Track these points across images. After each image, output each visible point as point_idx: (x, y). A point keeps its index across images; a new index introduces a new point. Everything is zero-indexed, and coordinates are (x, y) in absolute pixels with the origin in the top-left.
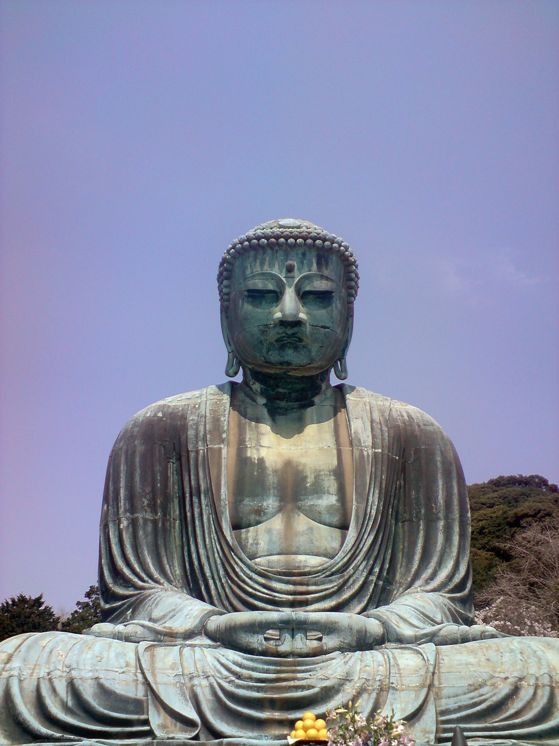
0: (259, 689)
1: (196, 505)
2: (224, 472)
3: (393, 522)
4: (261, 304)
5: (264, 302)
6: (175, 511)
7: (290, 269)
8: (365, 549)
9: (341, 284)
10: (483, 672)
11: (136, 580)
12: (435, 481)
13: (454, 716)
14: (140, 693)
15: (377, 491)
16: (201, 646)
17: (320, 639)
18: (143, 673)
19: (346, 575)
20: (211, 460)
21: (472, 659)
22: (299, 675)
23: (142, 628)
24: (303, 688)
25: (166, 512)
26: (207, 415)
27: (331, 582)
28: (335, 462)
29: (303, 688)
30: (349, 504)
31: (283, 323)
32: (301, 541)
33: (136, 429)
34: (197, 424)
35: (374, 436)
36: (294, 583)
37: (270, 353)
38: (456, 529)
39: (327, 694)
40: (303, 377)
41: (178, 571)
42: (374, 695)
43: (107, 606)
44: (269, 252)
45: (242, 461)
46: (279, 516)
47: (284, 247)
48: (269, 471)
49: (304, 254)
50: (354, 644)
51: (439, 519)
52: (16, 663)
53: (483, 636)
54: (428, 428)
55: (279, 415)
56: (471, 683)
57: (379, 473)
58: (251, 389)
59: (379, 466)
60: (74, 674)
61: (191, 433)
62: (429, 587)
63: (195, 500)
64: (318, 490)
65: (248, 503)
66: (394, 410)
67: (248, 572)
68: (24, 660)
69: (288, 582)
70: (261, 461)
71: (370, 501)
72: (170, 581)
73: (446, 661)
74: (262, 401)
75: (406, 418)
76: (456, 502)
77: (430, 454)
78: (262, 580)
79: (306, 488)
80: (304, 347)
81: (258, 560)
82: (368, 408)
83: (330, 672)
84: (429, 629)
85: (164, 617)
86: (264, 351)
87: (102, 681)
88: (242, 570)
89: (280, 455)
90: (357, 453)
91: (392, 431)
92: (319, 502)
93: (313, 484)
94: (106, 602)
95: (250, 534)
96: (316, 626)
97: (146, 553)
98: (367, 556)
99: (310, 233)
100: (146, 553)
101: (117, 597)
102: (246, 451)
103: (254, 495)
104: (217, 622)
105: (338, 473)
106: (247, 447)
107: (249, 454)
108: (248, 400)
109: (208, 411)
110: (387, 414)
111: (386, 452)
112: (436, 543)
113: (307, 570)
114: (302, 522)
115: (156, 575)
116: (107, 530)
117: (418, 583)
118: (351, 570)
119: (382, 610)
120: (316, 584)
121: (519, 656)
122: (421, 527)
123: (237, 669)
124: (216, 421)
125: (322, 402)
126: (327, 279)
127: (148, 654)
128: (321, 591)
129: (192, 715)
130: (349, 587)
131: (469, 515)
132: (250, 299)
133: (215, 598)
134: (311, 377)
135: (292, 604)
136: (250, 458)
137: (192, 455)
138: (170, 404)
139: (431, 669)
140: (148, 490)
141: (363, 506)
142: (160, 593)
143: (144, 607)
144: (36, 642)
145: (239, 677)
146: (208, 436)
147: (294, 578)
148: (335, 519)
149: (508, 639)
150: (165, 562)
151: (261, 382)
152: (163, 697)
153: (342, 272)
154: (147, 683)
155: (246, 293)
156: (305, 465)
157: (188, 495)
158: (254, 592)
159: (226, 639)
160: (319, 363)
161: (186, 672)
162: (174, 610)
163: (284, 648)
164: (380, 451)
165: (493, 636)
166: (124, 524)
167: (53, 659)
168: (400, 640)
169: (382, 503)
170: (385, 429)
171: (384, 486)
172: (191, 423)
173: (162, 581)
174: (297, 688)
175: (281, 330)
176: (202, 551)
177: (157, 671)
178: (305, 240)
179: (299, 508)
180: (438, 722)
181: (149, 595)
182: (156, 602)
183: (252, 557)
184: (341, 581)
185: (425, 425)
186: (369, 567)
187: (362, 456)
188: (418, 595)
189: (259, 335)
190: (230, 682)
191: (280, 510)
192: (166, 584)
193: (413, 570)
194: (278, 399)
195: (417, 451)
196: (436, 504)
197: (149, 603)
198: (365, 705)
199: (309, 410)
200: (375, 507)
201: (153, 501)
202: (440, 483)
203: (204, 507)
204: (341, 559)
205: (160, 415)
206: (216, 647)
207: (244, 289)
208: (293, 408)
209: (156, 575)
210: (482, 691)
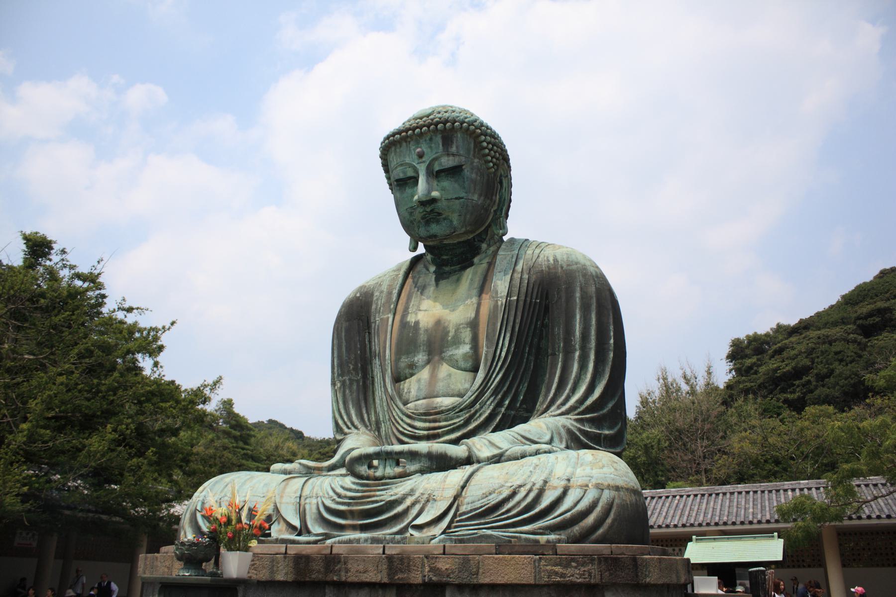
0: (348, 504)
2: (389, 337)
3: (532, 358)
9: (471, 156)
10: (495, 483)
12: (574, 316)
13: (464, 517)
15: (508, 335)
19: (473, 410)
22: (378, 493)
23: (298, 466)
24: (377, 502)
27: (458, 417)
28: (473, 315)
29: (377, 502)
31: (422, 203)
32: (440, 386)
36: (430, 421)
38: (592, 357)
40: (459, 243)
44: (404, 144)
45: (404, 324)
46: (428, 367)
47: (414, 137)
48: (422, 332)
49: (431, 139)
51: (575, 350)
54: (570, 268)
55: (443, 279)
56: (484, 491)
57: (512, 319)
59: (513, 313)
61: (374, 307)
62: (559, 412)
64: (457, 342)
65: (404, 361)
66: (542, 256)
67: (401, 415)
69: (425, 421)
71: (500, 345)
72: (366, 426)
75: (552, 261)
78: (408, 421)
80: (445, 219)
82: (514, 260)
86: (416, 229)
90: (492, 303)
91: (533, 278)
92: (456, 352)
93: (453, 337)
95: (405, 385)
96: (401, 454)
97: (351, 406)
98: (495, 392)
99: (432, 120)
100: (351, 406)
105: (474, 325)
107: (409, 319)
108: (424, 270)
110: (531, 263)
111: (522, 298)
114: (445, 369)
115: (356, 422)
117: (553, 408)
118: (477, 406)
120: (446, 420)
121: (531, 469)
124: (390, 293)
125: (481, 260)
126: (453, 155)
127: (284, 483)
128: (450, 425)
129: (297, 523)
130: (476, 420)
134: (467, 242)
135: (428, 438)
137: (373, 325)
139: (462, 483)
140: (352, 357)
144: (222, 479)
148: (469, 365)
149: (583, 452)
150: (364, 411)
153: (472, 145)
156: (449, 322)
160: (464, 229)
161: (304, 494)
163: (379, 473)
164: (515, 298)
165: (545, 452)
169: (513, 345)
170: (526, 276)
171: (517, 329)
173: (359, 426)
174: (373, 502)
175: (420, 210)
179: (443, 359)
183: (405, 403)
185: (568, 265)
186: (496, 401)
188: (537, 420)
190: (334, 500)
191: (428, 362)
192: (362, 429)
193: (549, 398)
194: (444, 265)
198: (414, 511)
199: (468, 270)
200: (505, 350)
201: (356, 365)
202: (578, 317)
204: (468, 398)
205: (358, 295)
208: (455, 271)
209: (356, 422)
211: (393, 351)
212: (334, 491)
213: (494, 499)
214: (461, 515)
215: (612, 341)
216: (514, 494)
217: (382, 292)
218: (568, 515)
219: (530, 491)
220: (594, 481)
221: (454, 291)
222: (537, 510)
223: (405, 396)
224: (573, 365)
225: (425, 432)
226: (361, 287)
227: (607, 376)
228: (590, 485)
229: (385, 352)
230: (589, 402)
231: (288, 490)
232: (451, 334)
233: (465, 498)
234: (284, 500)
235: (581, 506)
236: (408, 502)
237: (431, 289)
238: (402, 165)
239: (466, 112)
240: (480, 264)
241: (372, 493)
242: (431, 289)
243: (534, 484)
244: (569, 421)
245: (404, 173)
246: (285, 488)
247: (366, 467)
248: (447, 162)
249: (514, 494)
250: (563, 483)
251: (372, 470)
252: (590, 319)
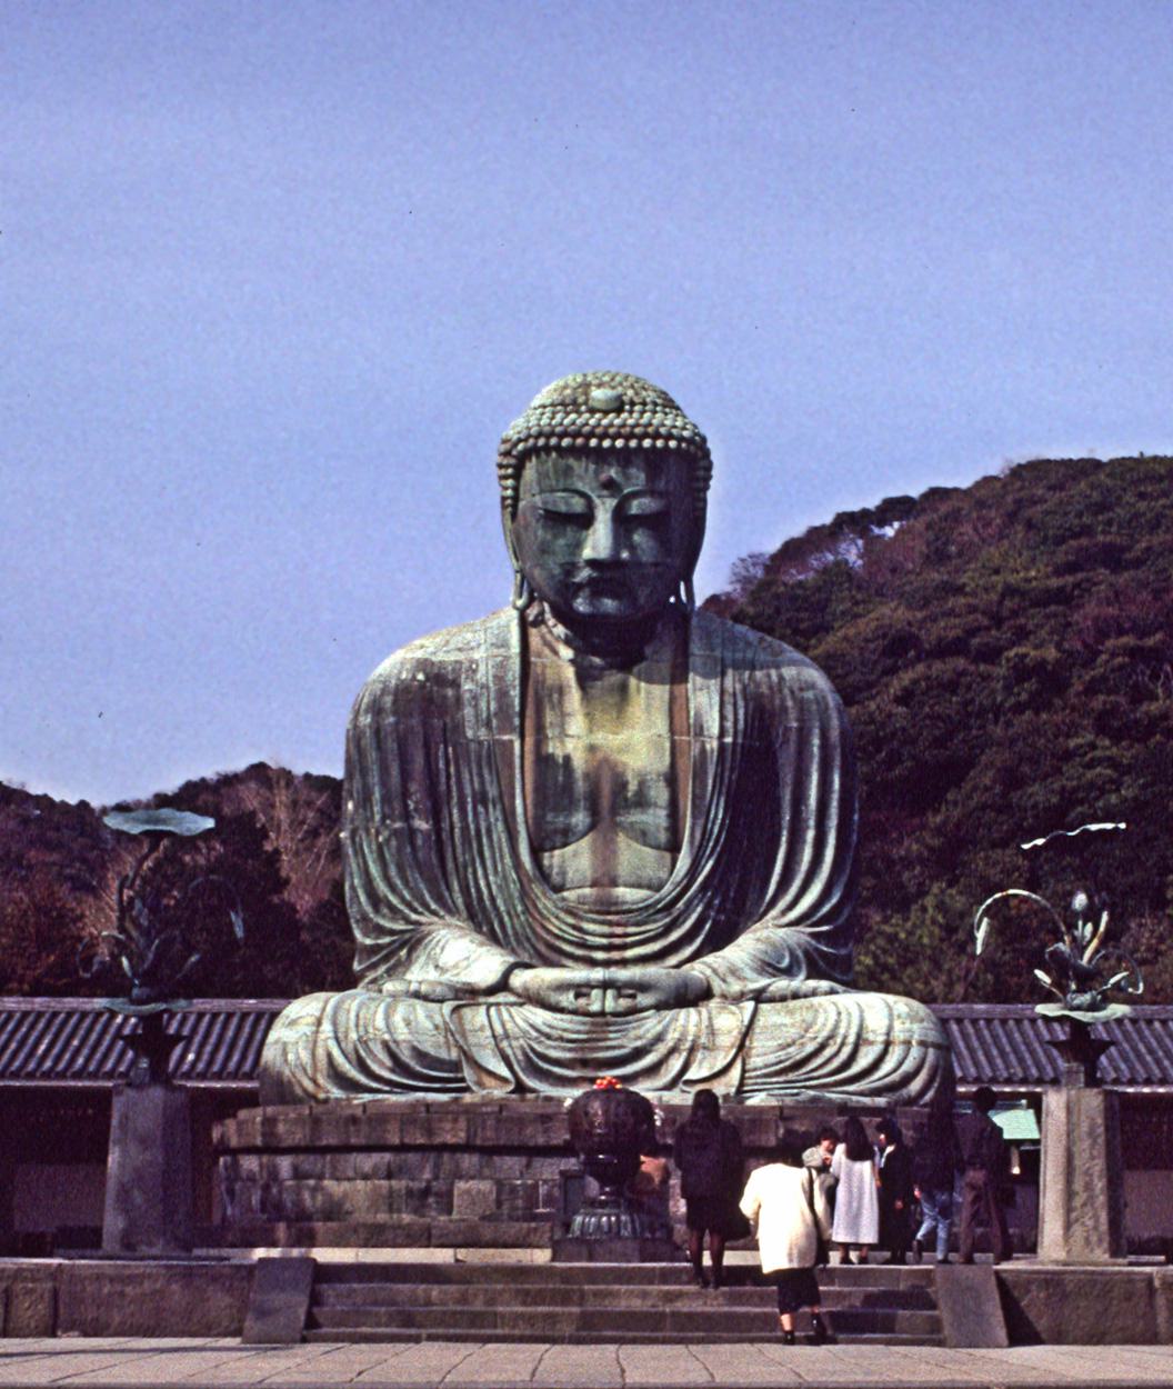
1: (482, 817)
4: (565, 530)
5: (569, 529)
8: (700, 879)
11: (407, 911)
12: (808, 775)
13: (759, 1073)
14: (454, 1054)
16: (506, 1004)
17: (633, 996)
18: (453, 1035)
19: (675, 912)
21: (787, 1020)
22: (611, 1035)
24: (613, 1048)
26: (491, 685)
27: (655, 921)
28: (667, 760)
29: (613, 1048)
30: (681, 824)
33: (388, 700)
34: (475, 698)
35: (723, 718)
36: (610, 924)
37: (579, 600)
39: (638, 1053)
41: (460, 902)
42: (685, 1054)
43: (368, 942)
50: (672, 1001)
51: (808, 828)
52: (327, 1027)
53: (814, 993)
58: (551, 632)
60: (387, 1037)
61: (468, 711)
63: (480, 809)
64: (641, 801)
68: (335, 1024)
69: (603, 923)
70: (567, 759)
71: (712, 816)
73: (761, 1021)
74: (567, 653)
76: (835, 804)
78: (571, 920)
79: (626, 799)
81: (565, 894)
83: (640, 1032)
84: (762, 982)
85: (456, 966)
87: (416, 1043)
88: (546, 908)
89: (592, 749)
94: (366, 935)
95: (553, 859)
99: (633, 427)
101: (381, 931)
102: (547, 745)
103: (557, 809)
105: (671, 779)
106: (547, 737)
107: (551, 750)
108: (547, 651)
109: (491, 678)
111: (740, 740)
112: (801, 860)
113: (625, 907)
115: (433, 906)
116: (357, 839)
117: (774, 912)
120: (637, 924)
122: (784, 839)
123: (547, 1030)
124: (502, 694)
129: (505, 1072)
130: (679, 927)
131: (856, 817)
132: (550, 523)
133: (512, 939)
136: (552, 755)
137: (473, 746)
138: (434, 659)
139: (744, 1030)
141: (701, 822)
142: (443, 932)
143: (426, 945)
145: (548, 1037)
146: (494, 722)
147: (609, 917)
151: (566, 625)
152: (477, 1058)
154: (461, 1048)
155: (541, 512)
156: (625, 764)
157: (469, 800)
158: (560, 933)
162: (467, 958)
163: (595, 1007)
166: (386, 833)
167: (361, 1022)
168: (724, 996)
170: (741, 703)
172: (467, 696)
173: (442, 913)
176: (491, 878)
177: (468, 1034)
178: (628, 438)
180: (743, 1078)
181: (429, 934)
182: (441, 944)
184: (667, 920)
187: (703, 751)
189: (562, 577)
191: (592, 827)
192: (447, 917)
195: (787, 729)
196: (807, 806)
203: (492, 820)
205: (421, 677)
206: (521, 1005)
207: (540, 505)
209: (433, 906)
210: (791, 1050)
211: (529, 801)
212: (538, 1030)
213: (796, 1053)
214: (749, 1071)
215: (856, 817)
216: (822, 1047)
217: (485, 687)
218: (895, 1077)
219: (843, 1044)
220: (916, 1037)
222: (855, 1069)
223: (556, 879)
224: (803, 849)
225: (604, 941)
226: (423, 664)
227: (848, 871)
228: (914, 1043)
229: (513, 797)
230: (826, 909)
231: (468, 1027)
232: (633, 787)
233: (750, 1048)
234: (472, 1040)
235: (908, 1066)
236: (661, 1049)
238: (564, 490)
239: (669, 404)
241: (603, 1036)
242: (574, 697)
243: (845, 1037)
244: (799, 936)
245: (567, 503)
246: (461, 1023)
247: (571, 995)
249: (822, 1047)
250: (881, 1038)
251: (582, 1001)
252: (832, 782)
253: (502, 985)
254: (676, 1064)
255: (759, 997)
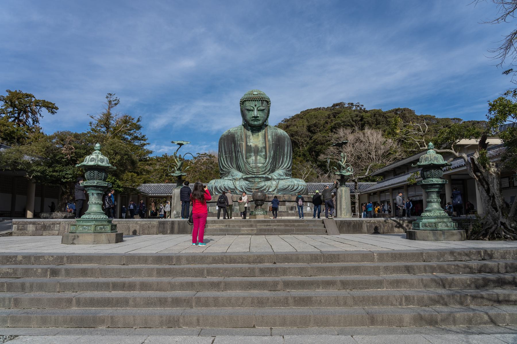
6: (234, 154)
7: (255, 106)
20: (240, 145)
25: (232, 155)
31: (254, 117)
32: (258, 161)
45: (247, 145)
64: (261, 152)
65: (248, 154)
73: (280, 183)
77: (284, 142)
96: (260, 177)
101: (224, 171)
104: (244, 177)
114: (259, 157)
119: (271, 174)
124: (241, 136)
159: (246, 179)
183: (249, 164)
197: (231, 172)
204: (265, 165)
213: (285, 187)
221: (258, 138)
236: (265, 187)
237: (251, 137)
240: (263, 132)
248: (262, 108)
253: (242, 178)
254: (267, 189)
255: (279, 179)
